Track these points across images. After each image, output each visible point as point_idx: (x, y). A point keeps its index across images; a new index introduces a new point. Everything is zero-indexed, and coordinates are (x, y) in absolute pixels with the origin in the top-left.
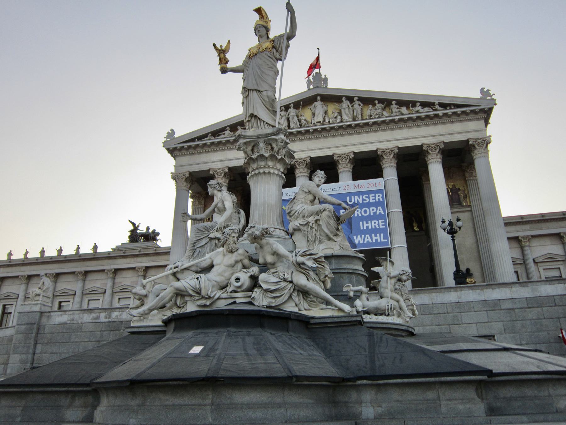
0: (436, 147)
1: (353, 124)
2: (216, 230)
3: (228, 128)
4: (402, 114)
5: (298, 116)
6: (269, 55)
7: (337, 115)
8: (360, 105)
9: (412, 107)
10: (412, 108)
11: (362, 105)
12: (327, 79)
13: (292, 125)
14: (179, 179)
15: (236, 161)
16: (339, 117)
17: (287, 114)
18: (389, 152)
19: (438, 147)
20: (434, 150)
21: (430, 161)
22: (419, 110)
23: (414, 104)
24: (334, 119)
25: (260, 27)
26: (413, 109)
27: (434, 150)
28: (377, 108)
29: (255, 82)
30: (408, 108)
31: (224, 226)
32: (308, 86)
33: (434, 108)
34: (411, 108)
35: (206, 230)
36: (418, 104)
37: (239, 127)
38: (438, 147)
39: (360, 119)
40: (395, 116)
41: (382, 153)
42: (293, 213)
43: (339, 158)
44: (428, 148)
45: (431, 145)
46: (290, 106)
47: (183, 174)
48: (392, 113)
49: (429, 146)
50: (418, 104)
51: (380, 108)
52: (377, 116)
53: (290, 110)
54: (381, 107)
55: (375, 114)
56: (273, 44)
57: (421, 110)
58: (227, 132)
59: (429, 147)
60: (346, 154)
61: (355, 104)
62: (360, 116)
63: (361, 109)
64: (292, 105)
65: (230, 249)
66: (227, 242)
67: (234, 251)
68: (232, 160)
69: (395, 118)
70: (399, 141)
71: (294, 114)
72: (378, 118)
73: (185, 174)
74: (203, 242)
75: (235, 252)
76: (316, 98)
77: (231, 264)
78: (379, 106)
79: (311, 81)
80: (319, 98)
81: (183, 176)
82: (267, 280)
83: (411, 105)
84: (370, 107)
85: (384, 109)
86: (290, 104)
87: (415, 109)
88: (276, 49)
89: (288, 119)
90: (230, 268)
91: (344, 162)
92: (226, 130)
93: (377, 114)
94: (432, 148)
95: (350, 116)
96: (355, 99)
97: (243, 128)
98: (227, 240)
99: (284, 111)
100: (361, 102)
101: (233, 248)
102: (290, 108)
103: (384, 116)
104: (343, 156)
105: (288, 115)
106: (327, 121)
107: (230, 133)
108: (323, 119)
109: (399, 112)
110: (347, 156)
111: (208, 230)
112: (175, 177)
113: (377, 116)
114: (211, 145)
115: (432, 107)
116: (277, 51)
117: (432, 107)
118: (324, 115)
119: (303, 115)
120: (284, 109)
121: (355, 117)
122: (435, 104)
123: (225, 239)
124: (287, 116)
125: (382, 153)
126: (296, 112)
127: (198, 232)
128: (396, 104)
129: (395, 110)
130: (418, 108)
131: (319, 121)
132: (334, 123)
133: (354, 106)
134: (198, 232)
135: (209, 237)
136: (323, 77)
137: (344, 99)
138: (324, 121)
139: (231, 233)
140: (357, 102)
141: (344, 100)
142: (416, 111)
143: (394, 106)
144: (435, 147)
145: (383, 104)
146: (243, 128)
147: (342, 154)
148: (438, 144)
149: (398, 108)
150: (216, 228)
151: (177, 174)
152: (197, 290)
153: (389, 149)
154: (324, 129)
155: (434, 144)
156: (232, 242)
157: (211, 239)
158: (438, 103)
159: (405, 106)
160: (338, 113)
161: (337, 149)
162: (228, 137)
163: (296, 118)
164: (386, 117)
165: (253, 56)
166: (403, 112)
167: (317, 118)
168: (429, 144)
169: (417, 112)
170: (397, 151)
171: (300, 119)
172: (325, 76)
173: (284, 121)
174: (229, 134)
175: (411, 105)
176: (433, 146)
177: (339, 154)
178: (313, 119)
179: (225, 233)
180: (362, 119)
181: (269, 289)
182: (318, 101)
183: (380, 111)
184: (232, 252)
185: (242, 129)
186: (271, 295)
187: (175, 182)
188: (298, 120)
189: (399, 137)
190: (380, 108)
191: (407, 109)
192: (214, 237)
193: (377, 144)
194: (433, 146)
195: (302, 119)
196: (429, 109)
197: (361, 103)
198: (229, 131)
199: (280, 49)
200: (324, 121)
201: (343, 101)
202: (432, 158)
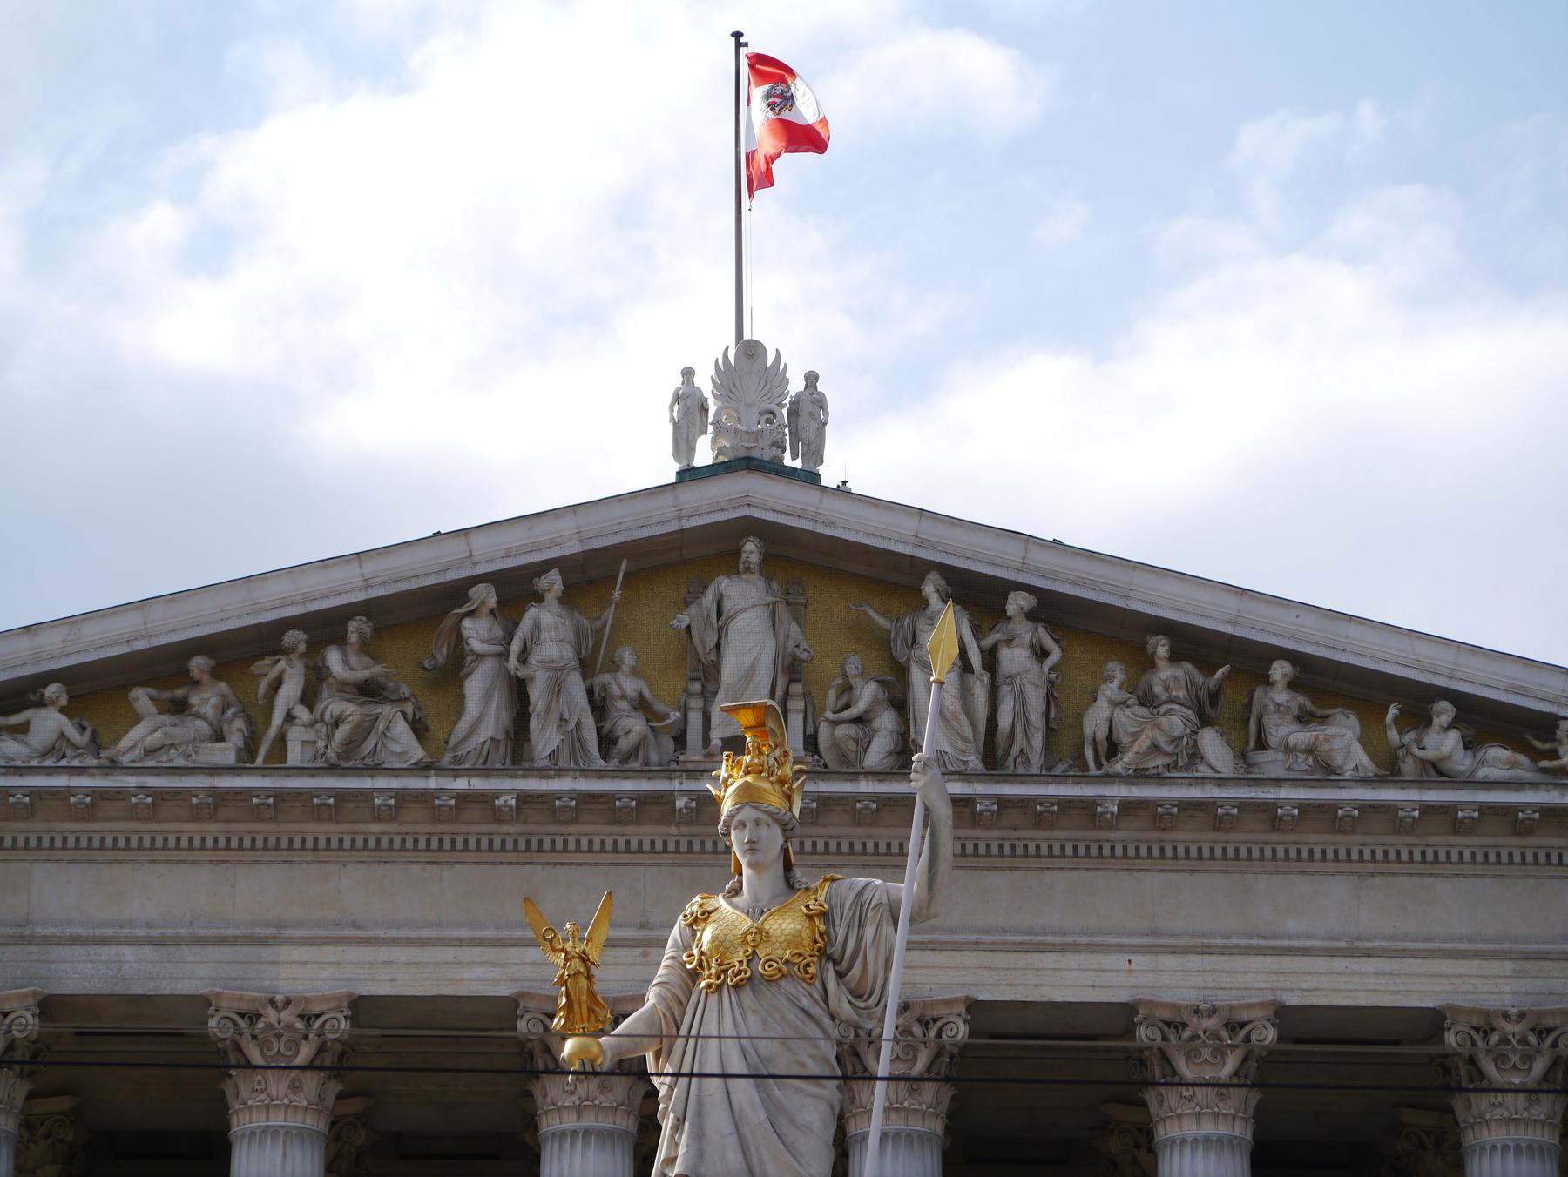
0: (1532, 1039)
1: (984, 797)
3: (52, 690)
4: (1326, 772)
5: (586, 667)
6: (805, 1002)
7: (875, 701)
8: (1041, 654)
9: (1403, 723)
10: (1400, 733)
11: (1055, 655)
12: (821, 403)
13: (545, 739)
15: (105, 952)
16: (886, 721)
17: (516, 647)
18: (1215, 1035)
19: (1550, 1040)
20: (1514, 1059)
21: (1487, 1136)
22: (1449, 757)
25: (757, 823)
26: (1409, 737)
27: (1514, 1059)
28: (1158, 689)
29: (740, 1157)
32: (683, 444)
34: (1393, 735)
36: (1444, 712)
38: (1550, 1040)
39: (1036, 759)
40: (1278, 782)
41: (1165, 1038)
44: (1478, 1038)
45: (1502, 1023)
46: (543, 582)
48: (1262, 745)
49: (1485, 1023)
50: (1444, 712)
51: (1181, 694)
52: (1160, 761)
53: (532, 612)
54: (1191, 687)
55: (1143, 743)
56: (821, 935)
57: (1462, 762)
58: (48, 723)
59: (1486, 1034)
60: (917, 1012)
61: (1009, 642)
62: (1038, 740)
63: (1051, 682)
64: (553, 582)
68: (75, 941)
69: (1284, 793)
70: (1287, 963)
72: (1158, 779)
76: (737, 553)
78: (1169, 676)
79: (704, 409)
80: (751, 550)
83: (1392, 712)
84: (1110, 679)
85: (1205, 712)
88: (835, 963)
89: (518, 690)
92: (41, 704)
93: (1155, 748)
94: (1505, 1041)
95: (967, 731)
96: (1017, 603)
100: (1054, 626)
102: (539, 598)
103: (1203, 771)
109: (1311, 751)
110: (920, 1021)
113: (1160, 761)
115: (1537, 744)
116: (840, 975)
117: (1537, 744)
120: (492, 601)
121: (1001, 740)
124: (513, 661)
125: (1165, 1038)
128: (1293, 685)
129: (1281, 730)
130: (1443, 742)
132: (854, 777)
133: (1005, 653)
136: (796, 385)
137: (930, 588)
140: (1024, 631)
141: (934, 601)
143: (1281, 696)
144: (1523, 1041)
145: (1207, 666)
148: (1550, 1023)
149: (1304, 719)
153: (1213, 1011)
155: (1522, 1016)
160: (882, 683)
162: (50, 771)
163: (576, 687)
164: (1221, 782)
165: (719, 987)
166: (1338, 759)
168: (1486, 1014)
169: (1437, 772)
170: (1271, 1035)
171: (605, 688)
172: (811, 378)
173: (487, 696)
174: (62, 735)
175: (1392, 712)
176: (1510, 1028)
180: (1047, 776)
182: (748, 570)
183: (1176, 722)
188: (590, 692)
190: (1181, 694)
193: (1133, 958)
194: (1510, 1028)
195: (615, 690)
196: (1514, 765)
197: (1049, 643)
198: (62, 710)
199: (856, 971)
201: (925, 603)
202: (1498, 1113)
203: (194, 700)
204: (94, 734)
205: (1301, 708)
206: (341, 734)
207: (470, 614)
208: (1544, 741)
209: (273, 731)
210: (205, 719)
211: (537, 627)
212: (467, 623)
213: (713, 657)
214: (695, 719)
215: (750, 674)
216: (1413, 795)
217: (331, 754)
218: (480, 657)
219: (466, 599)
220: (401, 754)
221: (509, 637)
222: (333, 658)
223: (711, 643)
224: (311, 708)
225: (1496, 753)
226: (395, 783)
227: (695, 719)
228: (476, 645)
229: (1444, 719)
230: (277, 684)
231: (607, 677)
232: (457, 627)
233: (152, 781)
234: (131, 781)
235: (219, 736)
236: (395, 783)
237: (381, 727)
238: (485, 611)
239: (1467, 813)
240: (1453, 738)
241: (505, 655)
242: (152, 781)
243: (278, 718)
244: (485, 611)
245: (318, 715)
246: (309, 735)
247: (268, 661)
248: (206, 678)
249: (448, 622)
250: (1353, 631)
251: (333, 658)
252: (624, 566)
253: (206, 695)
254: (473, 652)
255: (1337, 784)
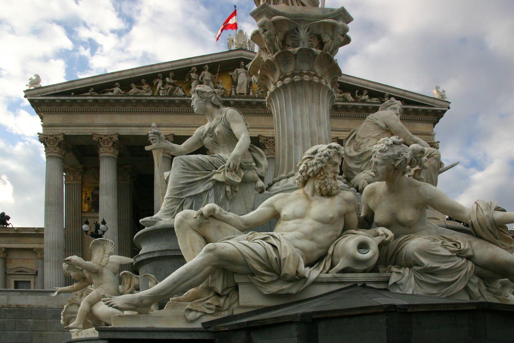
2: (226, 168)
4: (346, 100)
10: (358, 95)
14: (50, 142)
17: (200, 77)
23: (361, 90)
24: (261, 93)
26: (359, 96)
30: (353, 96)
31: (241, 164)
33: (383, 100)
35: (203, 167)
36: (366, 92)
37: (133, 85)
42: (367, 155)
43: (265, 142)
46: (205, 67)
47: (55, 136)
50: (366, 92)
53: (203, 72)
65: (329, 187)
66: (322, 173)
67: (334, 192)
69: (339, 103)
71: (210, 79)
73: (58, 137)
74: (201, 189)
75: (334, 195)
76: (240, 64)
77: (332, 218)
81: (55, 139)
82: (431, 250)
83: (357, 91)
86: (204, 65)
87: (361, 97)
90: (328, 225)
91: (272, 148)
97: (138, 87)
98: (321, 169)
99: (196, 73)
101: (334, 188)
102: (204, 70)
104: (271, 140)
105: (202, 79)
106: (251, 94)
107: (121, 91)
108: (247, 91)
109: (343, 97)
111: (213, 167)
112: (43, 139)
114: (94, 104)
115: (381, 98)
118: (248, 87)
119: (221, 81)
120: (196, 70)
122: (385, 96)
123: (319, 165)
124: (200, 79)
126: (211, 76)
127: (187, 169)
130: (365, 97)
131: (242, 92)
134: (187, 169)
135: (213, 180)
138: (248, 93)
139: (332, 155)
142: (361, 100)
146: (138, 87)
147: (270, 138)
150: (226, 165)
151: (47, 135)
152: (270, 264)
154: (248, 103)
156: (331, 175)
157: (217, 183)
158: (388, 95)
159: (349, 92)
161: (264, 130)
167: (240, 89)
169: (363, 101)
174: (119, 92)
175: (357, 91)
177: (266, 137)
178: (234, 89)
179: (318, 154)
181: (436, 268)
184: (329, 194)
185: (137, 88)
186: (435, 280)
187: (44, 146)
189: (340, 127)
191: (352, 96)
192: (223, 180)
196: (378, 100)
200: (248, 93)
203: (143, 87)
204: (125, 93)
205: (341, 92)
206: (169, 90)
207: (192, 72)
208: (382, 98)
209: (157, 91)
210: (145, 90)
211: (204, 74)
212: (191, 74)
213: (236, 81)
214: (233, 92)
215: (243, 83)
216: (361, 104)
217: (168, 94)
218: (194, 79)
219: (191, 70)
220: (180, 94)
221: (199, 77)
222: (168, 80)
223: (235, 78)
224: (164, 87)
225: (374, 99)
226: (179, 98)
227: (233, 92)
228: (193, 77)
229: (366, 93)
230: (157, 83)
231: (217, 85)
232: (190, 75)
233: (135, 98)
234: (132, 98)
235: (147, 92)
236: (179, 98)
237: (176, 90)
238: (195, 72)
239: (370, 108)
240: (367, 96)
241: (198, 80)
242: (135, 98)
243: (158, 89)
244: (195, 72)
245: (165, 88)
246: (163, 92)
247: (155, 80)
248: (145, 83)
249: (188, 75)
250: (350, 78)
251: (168, 80)
252: (219, 66)
253: (145, 86)
254: (193, 79)
255: (349, 102)
